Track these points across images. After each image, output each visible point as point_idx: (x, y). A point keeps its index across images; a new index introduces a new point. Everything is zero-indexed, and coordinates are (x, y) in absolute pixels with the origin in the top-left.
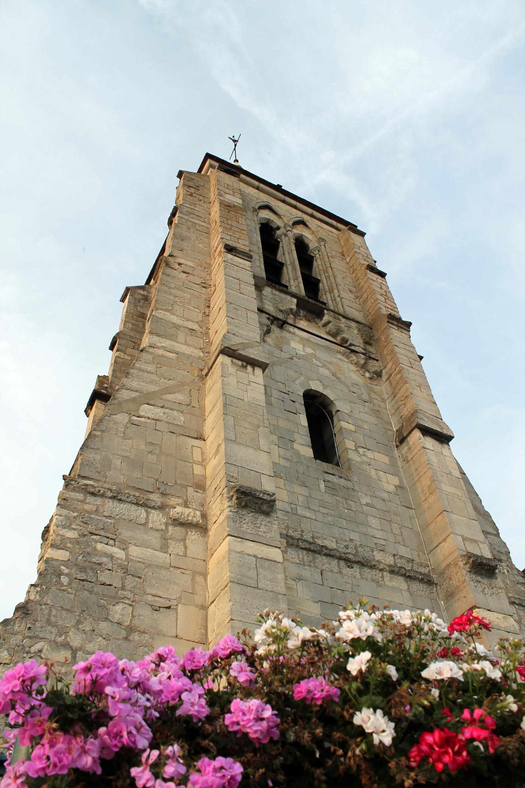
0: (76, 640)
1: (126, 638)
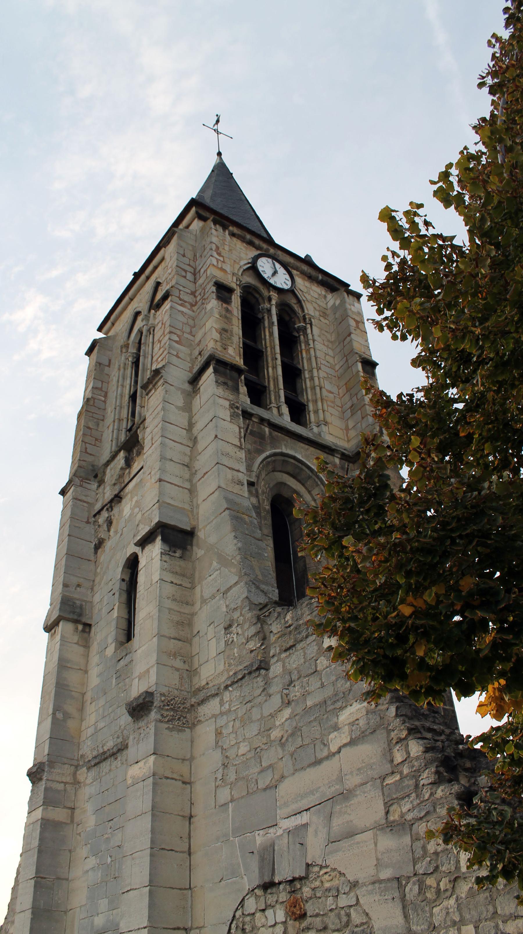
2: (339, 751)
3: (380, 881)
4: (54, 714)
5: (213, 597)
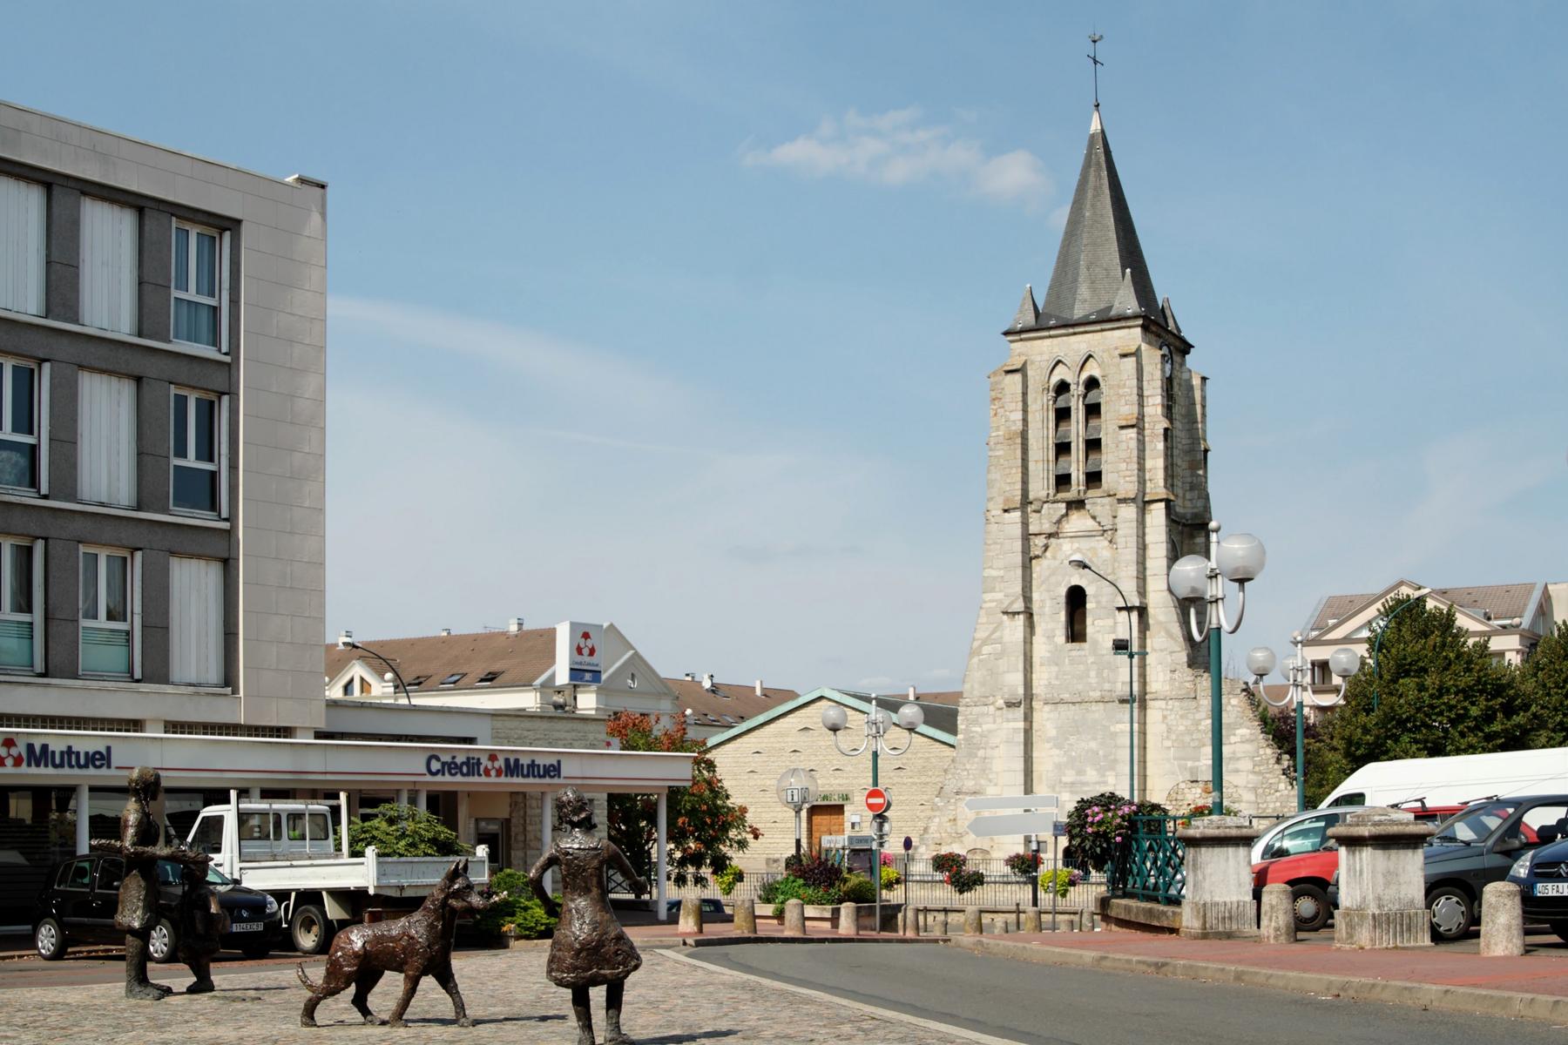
0: (968, 767)
2: (1235, 743)
5: (1162, 650)
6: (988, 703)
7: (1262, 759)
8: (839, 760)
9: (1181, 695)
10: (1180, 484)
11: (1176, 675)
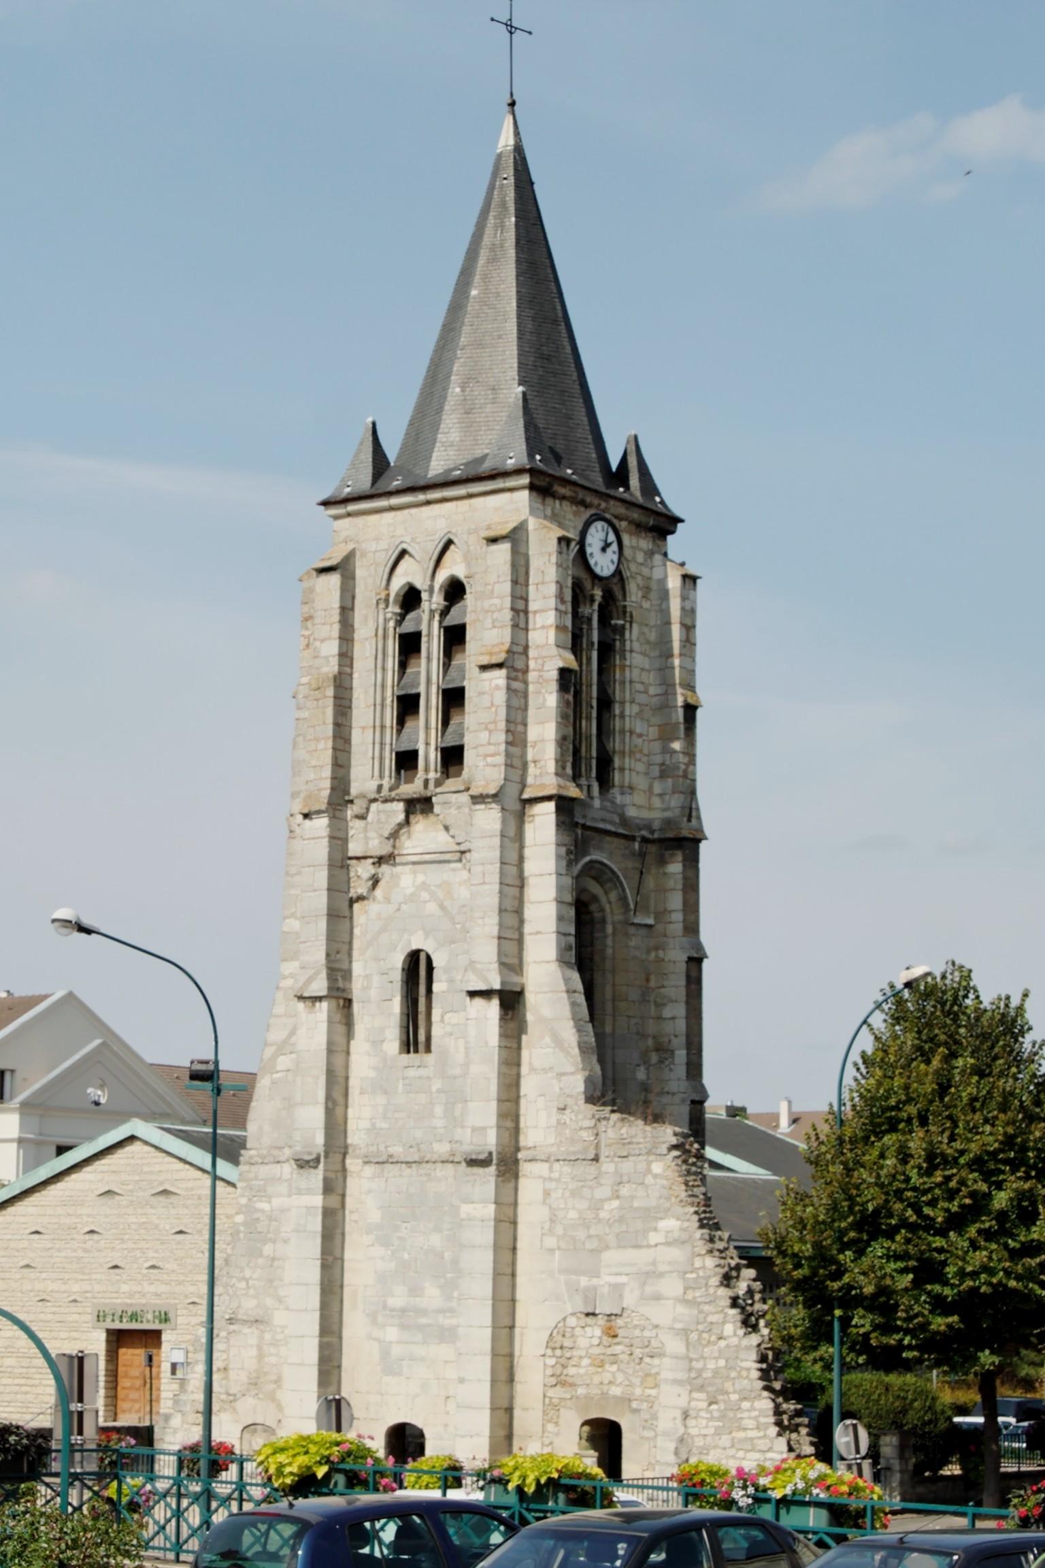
0: (247, 1273)
1: (271, 1266)
2: (656, 1245)
3: (673, 1329)
4: (326, 1103)
5: (545, 1071)
6: (281, 1159)
7: (698, 1277)
8: (157, 1252)
9: (574, 1153)
10: (640, 767)
11: (567, 1116)
